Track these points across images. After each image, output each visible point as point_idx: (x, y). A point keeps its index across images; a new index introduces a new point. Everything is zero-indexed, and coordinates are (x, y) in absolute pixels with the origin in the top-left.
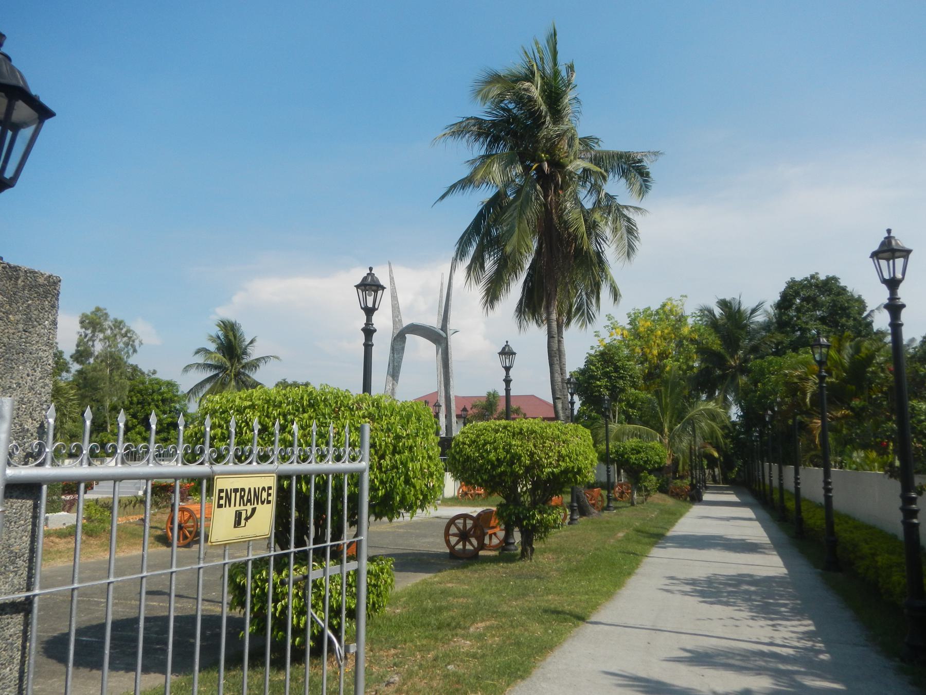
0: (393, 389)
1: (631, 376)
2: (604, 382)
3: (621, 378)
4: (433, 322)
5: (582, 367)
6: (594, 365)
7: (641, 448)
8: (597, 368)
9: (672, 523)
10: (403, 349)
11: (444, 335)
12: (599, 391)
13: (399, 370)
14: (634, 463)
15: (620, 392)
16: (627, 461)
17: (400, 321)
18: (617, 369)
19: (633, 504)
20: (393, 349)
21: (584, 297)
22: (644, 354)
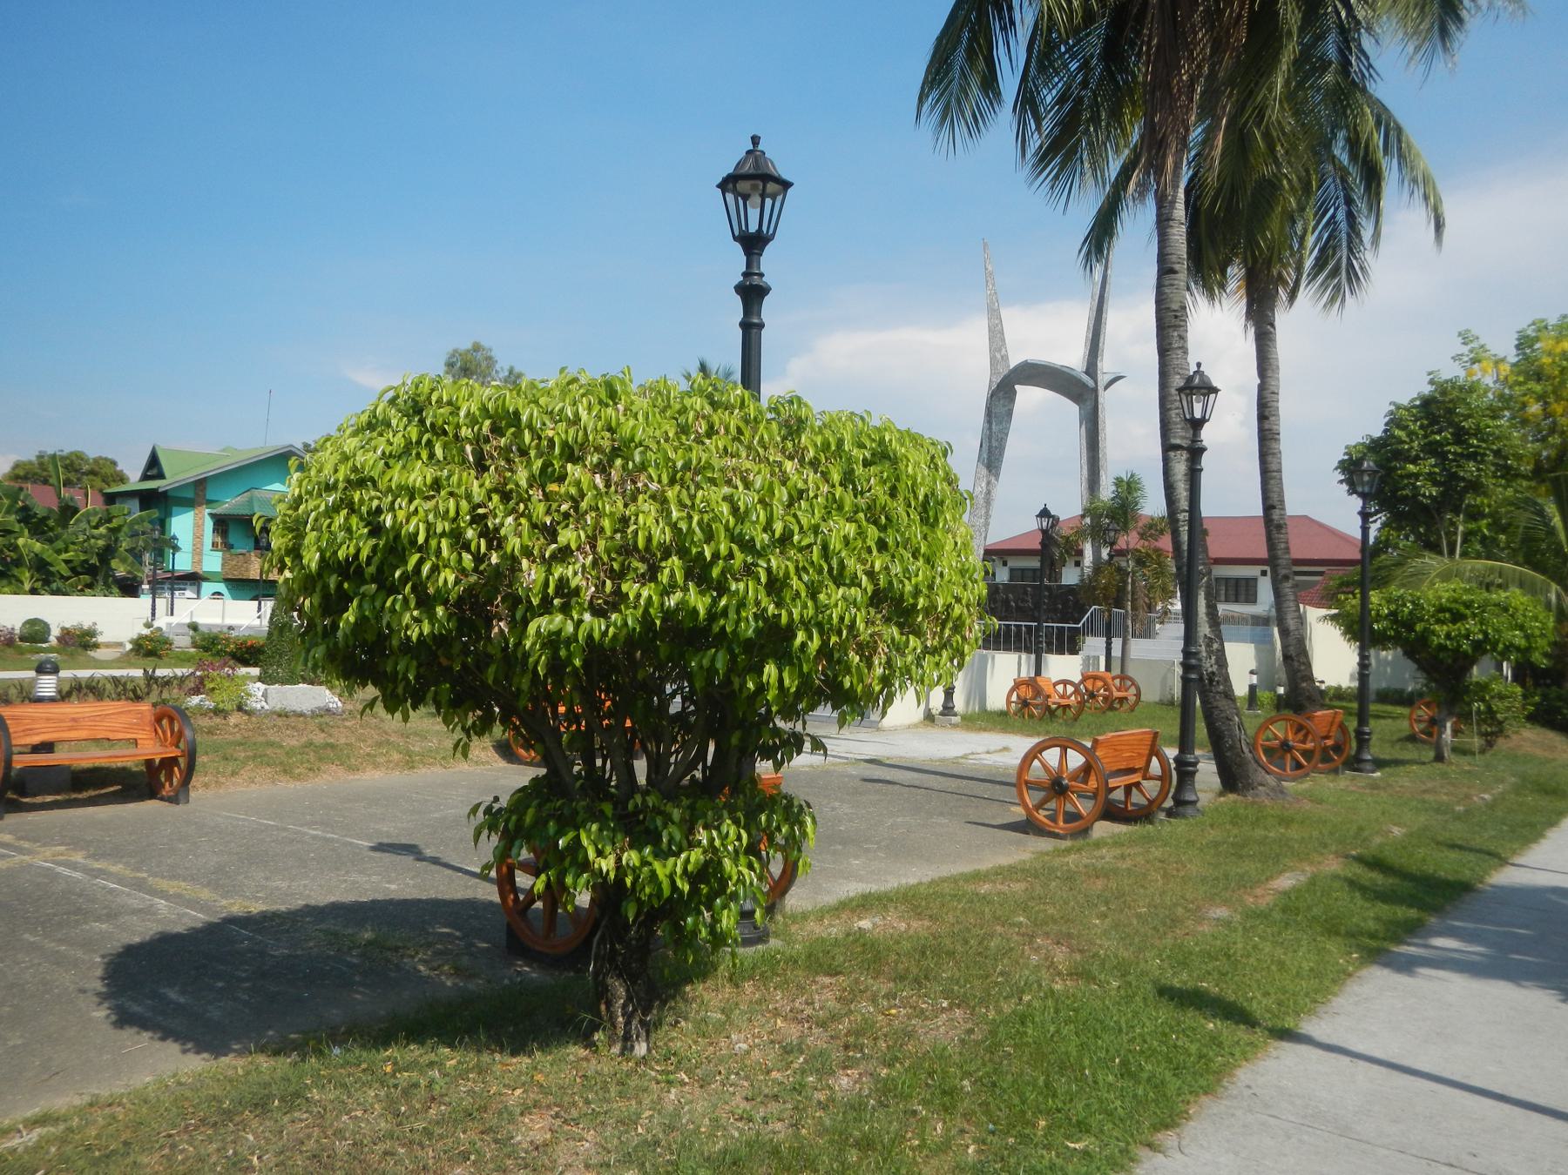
0: (989, 492)
1: (1497, 453)
2: (1429, 464)
3: (1473, 456)
4: (1072, 358)
5: (1377, 432)
6: (1404, 428)
7: (1468, 605)
8: (1411, 434)
9: (1530, 830)
10: (1010, 413)
11: (1091, 383)
12: (1415, 488)
13: (1001, 454)
14: (1442, 648)
15: (1465, 490)
16: (1424, 638)
17: (1005, 358)
18: (1460, 436)
19: (1439, 758)
20: (989, 414)
21: (1343, 226)
22: (1547, 414)
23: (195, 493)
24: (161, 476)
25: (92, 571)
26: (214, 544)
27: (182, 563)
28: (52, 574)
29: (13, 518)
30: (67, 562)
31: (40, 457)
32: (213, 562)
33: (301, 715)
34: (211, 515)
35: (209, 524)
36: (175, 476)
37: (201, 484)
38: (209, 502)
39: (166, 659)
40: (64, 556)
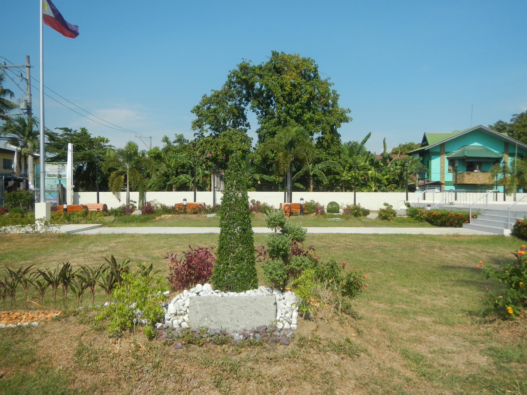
23: (441, 149)
24: (427, 144)
25: (397, 182)
26: (449, 170)
27: (435, 177)
28: (382, 183)
29: (367, 163)
30: (387, 179)
31: (400, 146)
32: (449, 177)
33: (222, 339)
34: (448, 158)
35: (447, 162)
36: (432, 143)
37: (442, 145)
38: (446, 153)
39: (392, 221)
40: (386, 177)
